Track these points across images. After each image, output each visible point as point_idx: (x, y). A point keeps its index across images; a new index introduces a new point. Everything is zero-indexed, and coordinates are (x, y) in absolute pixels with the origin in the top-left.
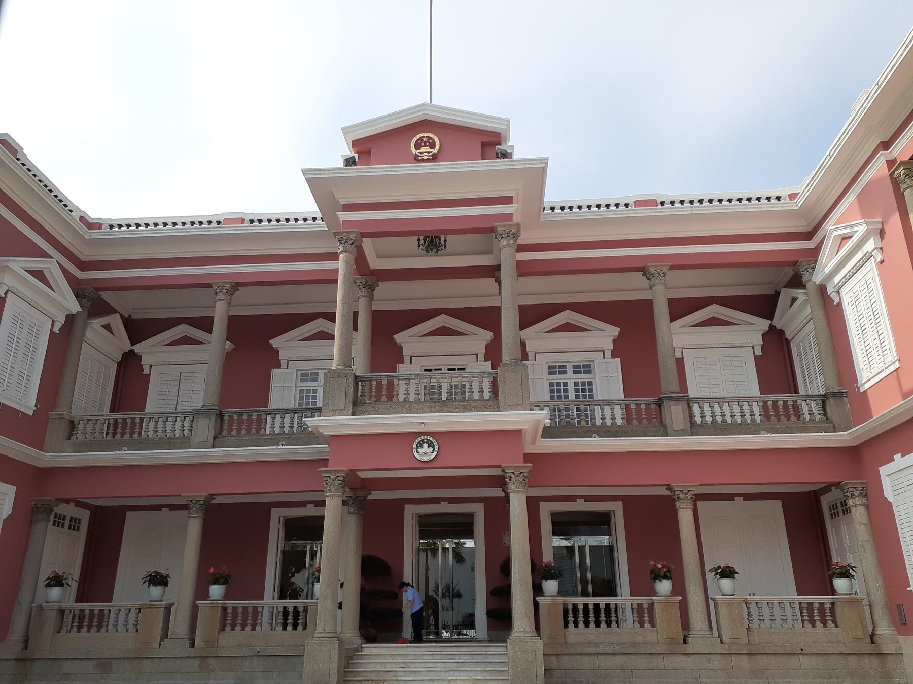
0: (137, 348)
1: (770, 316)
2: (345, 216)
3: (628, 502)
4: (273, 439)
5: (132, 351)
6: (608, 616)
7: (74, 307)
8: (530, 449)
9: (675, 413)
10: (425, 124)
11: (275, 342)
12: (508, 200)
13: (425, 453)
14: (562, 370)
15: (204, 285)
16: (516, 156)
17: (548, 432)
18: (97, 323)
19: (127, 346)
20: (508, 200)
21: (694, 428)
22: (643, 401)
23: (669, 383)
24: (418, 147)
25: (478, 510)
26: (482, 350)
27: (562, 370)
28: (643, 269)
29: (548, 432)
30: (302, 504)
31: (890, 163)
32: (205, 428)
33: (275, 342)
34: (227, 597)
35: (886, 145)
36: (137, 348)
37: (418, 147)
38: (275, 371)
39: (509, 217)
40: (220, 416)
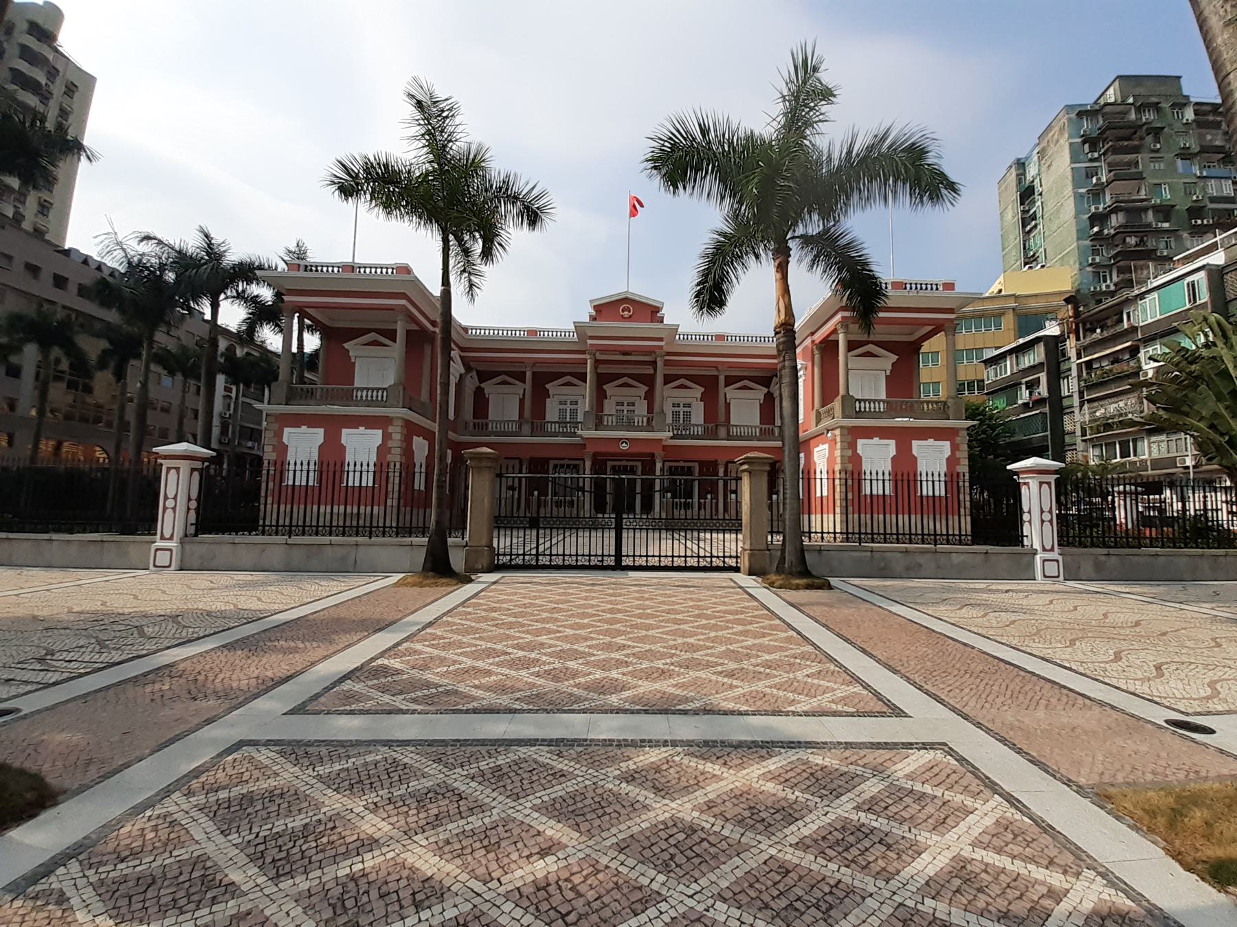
0: (483, 385)
1: (768, 386)
2: (590, 342)
3: (701, 463)
4: (555, 435)
5: (479, 387)
6: (687, 506)
7: (463, 371)
8: (664, 443)
9: (722, 431)
10: (626, 300)
11: (547, 386)
12: (661, 339)
13: (624, 447)
14: (679, 406)
15: (521, 362)
16: (665, 322)
17: (672, 438)
18: (469, 376)
19: (477, 383)
20: (661, 339)
21: (729, 437)
22: (710, 425)
23: (722, 418)
24: (623, 311)
25: (639, 464)
26: (643, 395)
27: (679, 406)
28: (716, 367)
29: (672, 438)
30: (563, 459)
31: (813, 342)
32: (526, 428)
33: (547, 386)
34: (539, 495)
35: (812, 334)
36: (483, 385)
37: (623, 311)
38: (548, 400)
39: (661, 347)
40: (532, 423)
